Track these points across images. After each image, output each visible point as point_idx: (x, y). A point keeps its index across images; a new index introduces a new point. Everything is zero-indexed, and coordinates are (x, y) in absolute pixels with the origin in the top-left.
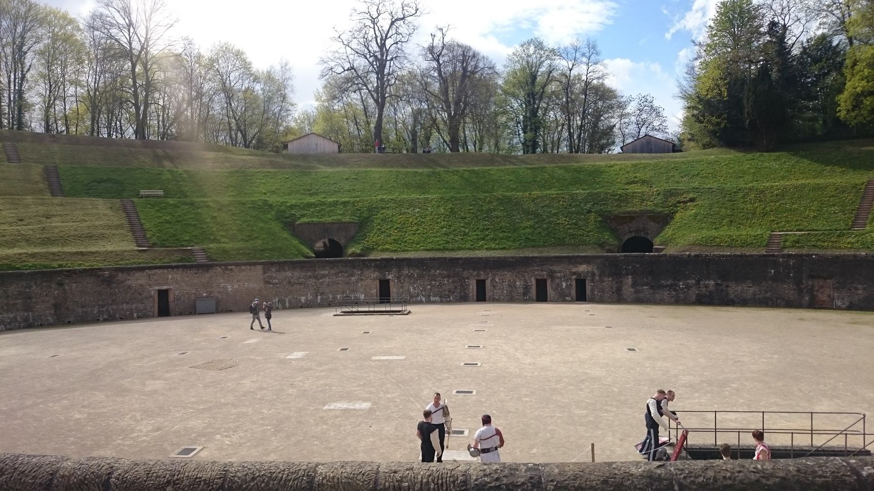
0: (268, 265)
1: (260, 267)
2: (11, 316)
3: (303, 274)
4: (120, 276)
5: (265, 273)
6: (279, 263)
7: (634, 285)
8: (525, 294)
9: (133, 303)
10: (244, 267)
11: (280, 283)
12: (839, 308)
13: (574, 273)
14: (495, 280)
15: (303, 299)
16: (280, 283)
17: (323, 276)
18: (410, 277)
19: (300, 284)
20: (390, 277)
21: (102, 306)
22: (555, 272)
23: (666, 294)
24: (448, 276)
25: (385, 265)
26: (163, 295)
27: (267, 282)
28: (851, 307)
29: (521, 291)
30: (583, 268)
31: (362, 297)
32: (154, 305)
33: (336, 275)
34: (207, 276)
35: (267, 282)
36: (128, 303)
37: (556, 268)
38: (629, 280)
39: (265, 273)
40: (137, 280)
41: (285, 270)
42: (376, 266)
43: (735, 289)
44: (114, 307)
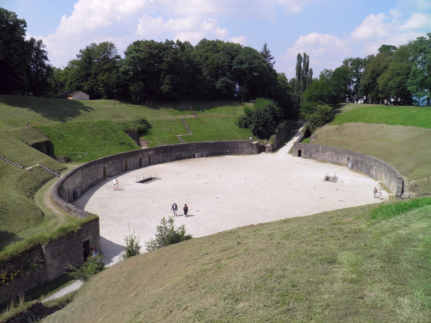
7: (162, 156)
8: (137, 165)
10: (78, 171)
12: (204, 157)
13: (149, 155)
14: (131, 161)
17: (92, 170)
18: (110, 164)
20: (106, 166)
22: (144, 155)
23: (169, 158)
24: (119, 162)
25: (105, 160)
27: (82, 177)
28: (207, 156)
29: (136, 164)
30: (151, 153)
31: (100, 176)
33: (94, 168)
37: (145, 154)
38: (161, 155)
42: (103, 162)
43: (184, 154)
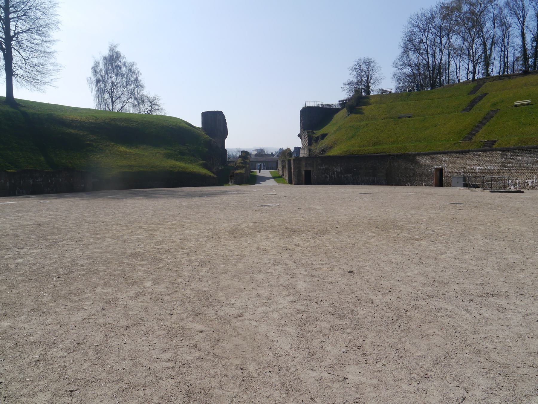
0: (504, 151)
1: (499, 153)
2: (368, 178)
3: (531, 159)
4: (418, 158)
5: (502, 157)
6: (513, 150)
9: (423, 177)
10: (488, 153)
11: (513, 167)
15: (530, 182)
16: (513, 167)
19: (527, 168)
21: (407, 177)
26: (441, 171)
27: (504, 166)
32: (432, 179)
34: (465, 159)
35: (504, 166)
36: (420, 177)
39: (502, 157)
40: (425, 161)
41: (517, 156)
44: (414, 178)
